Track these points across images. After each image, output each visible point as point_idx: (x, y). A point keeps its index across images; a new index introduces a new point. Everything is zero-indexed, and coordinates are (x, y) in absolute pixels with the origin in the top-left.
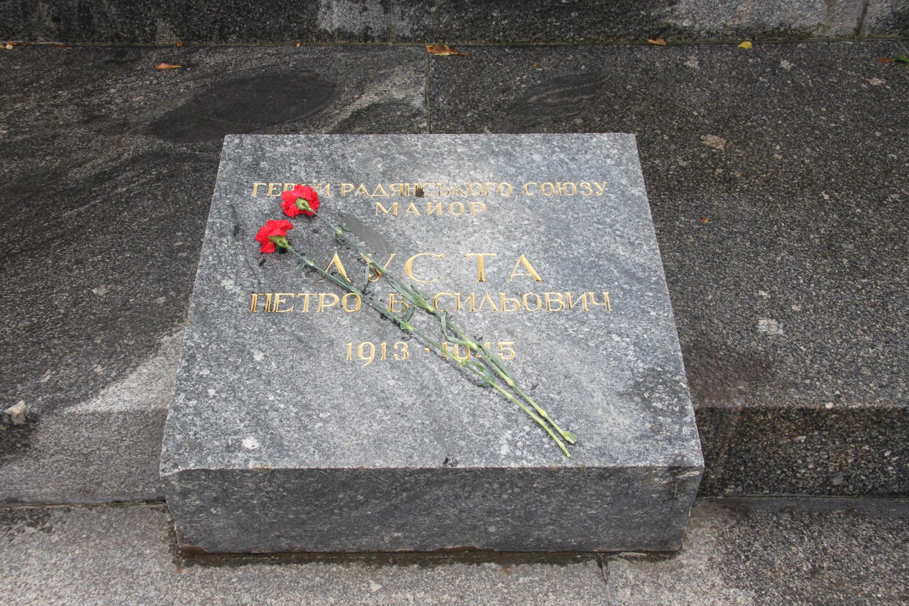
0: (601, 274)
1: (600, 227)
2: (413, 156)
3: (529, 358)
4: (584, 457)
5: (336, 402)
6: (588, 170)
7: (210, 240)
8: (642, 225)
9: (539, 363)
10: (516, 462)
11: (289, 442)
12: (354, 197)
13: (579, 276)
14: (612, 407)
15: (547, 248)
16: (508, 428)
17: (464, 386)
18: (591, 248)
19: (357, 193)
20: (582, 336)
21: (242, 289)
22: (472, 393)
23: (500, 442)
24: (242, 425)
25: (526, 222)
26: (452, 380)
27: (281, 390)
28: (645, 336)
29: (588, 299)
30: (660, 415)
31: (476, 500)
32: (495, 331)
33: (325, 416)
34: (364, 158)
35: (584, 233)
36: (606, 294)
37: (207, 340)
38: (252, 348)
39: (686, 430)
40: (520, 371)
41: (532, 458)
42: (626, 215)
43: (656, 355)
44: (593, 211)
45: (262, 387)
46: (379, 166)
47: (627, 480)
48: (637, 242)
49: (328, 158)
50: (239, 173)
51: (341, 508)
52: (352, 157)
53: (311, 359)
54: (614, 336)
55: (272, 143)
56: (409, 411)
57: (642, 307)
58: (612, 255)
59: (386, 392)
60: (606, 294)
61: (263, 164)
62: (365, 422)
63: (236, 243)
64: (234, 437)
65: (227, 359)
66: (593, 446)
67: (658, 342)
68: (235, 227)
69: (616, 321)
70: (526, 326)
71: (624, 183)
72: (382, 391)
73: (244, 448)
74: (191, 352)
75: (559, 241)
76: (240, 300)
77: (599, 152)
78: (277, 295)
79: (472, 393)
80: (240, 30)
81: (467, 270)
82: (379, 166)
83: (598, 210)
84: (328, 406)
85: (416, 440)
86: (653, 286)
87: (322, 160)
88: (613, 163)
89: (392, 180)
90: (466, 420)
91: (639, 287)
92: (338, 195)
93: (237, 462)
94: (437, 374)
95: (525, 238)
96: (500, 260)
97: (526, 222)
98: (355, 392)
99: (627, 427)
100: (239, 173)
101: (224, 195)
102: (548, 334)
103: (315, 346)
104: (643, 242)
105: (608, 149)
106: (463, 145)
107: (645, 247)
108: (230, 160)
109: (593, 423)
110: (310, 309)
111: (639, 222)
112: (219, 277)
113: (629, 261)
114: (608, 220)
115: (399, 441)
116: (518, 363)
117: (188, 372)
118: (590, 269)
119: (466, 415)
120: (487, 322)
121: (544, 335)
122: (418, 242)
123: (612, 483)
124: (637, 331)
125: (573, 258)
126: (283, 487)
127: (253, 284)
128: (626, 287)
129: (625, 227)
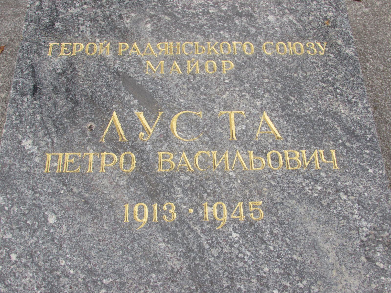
0: (327, 132)
1: (325, 85)
2: (175, 16)
5: (117, 266)
6: (311, 31)
7: (14, 100)
8: (356, 84)
9: (283, 224)
12: (129, 56)
14: (344, 268)
15: (284, 106)
17: (222, 248)
19: (131, 52)
20: (316, 195)
21: (38, 149)
22: (229, 255)
25: (267, 80)
26: (213, 242)
27: (71, 255)
28: (366, 194)
30: (382, 275)
32: (247, 191)
33: (108, 282)
34: (137, 18)
35: (313, 91)
36: (333, 152)
37: (10, 202)
38: (47, 210)
40: (268, 231)
42: (343, 74)
43: (376, 214)
44: (318, 70)
46: (149, 26)
48: (354, 100)
49: (108, 18)
50: (39, 33)
52: (127, 18)
53: (96, 221)
54: (341, 194)
55: (65, 5)
56: (178, 276)
57: (362, 164)
58: (335, 113)
59: (158, 255)
60: (333, 152)
62: (141, 288)
63: (35, 102)
68: (34, 86)
69: (342, 179)
70: (271, 185)
71: (339, 43)
72: (155, 255)
75: (293, 98)
76: (37, 160)
77: (318, 14)
78: (67, 154)
79: (229, 255)
81: (221, 128)
82: (149, 26)
83: (322, 69)
84: (109, 271)
86: (369, 144)
87: (104, 21)
90: (226, 285)
94: (200, 236)
96: (247, 118)
97: (267, 80)
98: (132, 256)
99: (357, 288)
100: (39, 33)
101: (26, 55)
102: (289, 193)
103: (98, 208)
104: (358, 101)
105: (325, 12)
106: (214, 7)
107: (360, 105)
108: (32, 21)
110: (94, 169)
111: (353, 81)
112: (20, 137)
113: (348, 119)
114: (330, 79)
116: (266, 224)
118: (319, 126)
119: (226, 279)
120: (239, 181)
121: (286, 194)
122: (181, 100)
124: (359, 189)
125: (306, 116)
127: (47, 144)
128: (348, 144)
129: (343, 85)
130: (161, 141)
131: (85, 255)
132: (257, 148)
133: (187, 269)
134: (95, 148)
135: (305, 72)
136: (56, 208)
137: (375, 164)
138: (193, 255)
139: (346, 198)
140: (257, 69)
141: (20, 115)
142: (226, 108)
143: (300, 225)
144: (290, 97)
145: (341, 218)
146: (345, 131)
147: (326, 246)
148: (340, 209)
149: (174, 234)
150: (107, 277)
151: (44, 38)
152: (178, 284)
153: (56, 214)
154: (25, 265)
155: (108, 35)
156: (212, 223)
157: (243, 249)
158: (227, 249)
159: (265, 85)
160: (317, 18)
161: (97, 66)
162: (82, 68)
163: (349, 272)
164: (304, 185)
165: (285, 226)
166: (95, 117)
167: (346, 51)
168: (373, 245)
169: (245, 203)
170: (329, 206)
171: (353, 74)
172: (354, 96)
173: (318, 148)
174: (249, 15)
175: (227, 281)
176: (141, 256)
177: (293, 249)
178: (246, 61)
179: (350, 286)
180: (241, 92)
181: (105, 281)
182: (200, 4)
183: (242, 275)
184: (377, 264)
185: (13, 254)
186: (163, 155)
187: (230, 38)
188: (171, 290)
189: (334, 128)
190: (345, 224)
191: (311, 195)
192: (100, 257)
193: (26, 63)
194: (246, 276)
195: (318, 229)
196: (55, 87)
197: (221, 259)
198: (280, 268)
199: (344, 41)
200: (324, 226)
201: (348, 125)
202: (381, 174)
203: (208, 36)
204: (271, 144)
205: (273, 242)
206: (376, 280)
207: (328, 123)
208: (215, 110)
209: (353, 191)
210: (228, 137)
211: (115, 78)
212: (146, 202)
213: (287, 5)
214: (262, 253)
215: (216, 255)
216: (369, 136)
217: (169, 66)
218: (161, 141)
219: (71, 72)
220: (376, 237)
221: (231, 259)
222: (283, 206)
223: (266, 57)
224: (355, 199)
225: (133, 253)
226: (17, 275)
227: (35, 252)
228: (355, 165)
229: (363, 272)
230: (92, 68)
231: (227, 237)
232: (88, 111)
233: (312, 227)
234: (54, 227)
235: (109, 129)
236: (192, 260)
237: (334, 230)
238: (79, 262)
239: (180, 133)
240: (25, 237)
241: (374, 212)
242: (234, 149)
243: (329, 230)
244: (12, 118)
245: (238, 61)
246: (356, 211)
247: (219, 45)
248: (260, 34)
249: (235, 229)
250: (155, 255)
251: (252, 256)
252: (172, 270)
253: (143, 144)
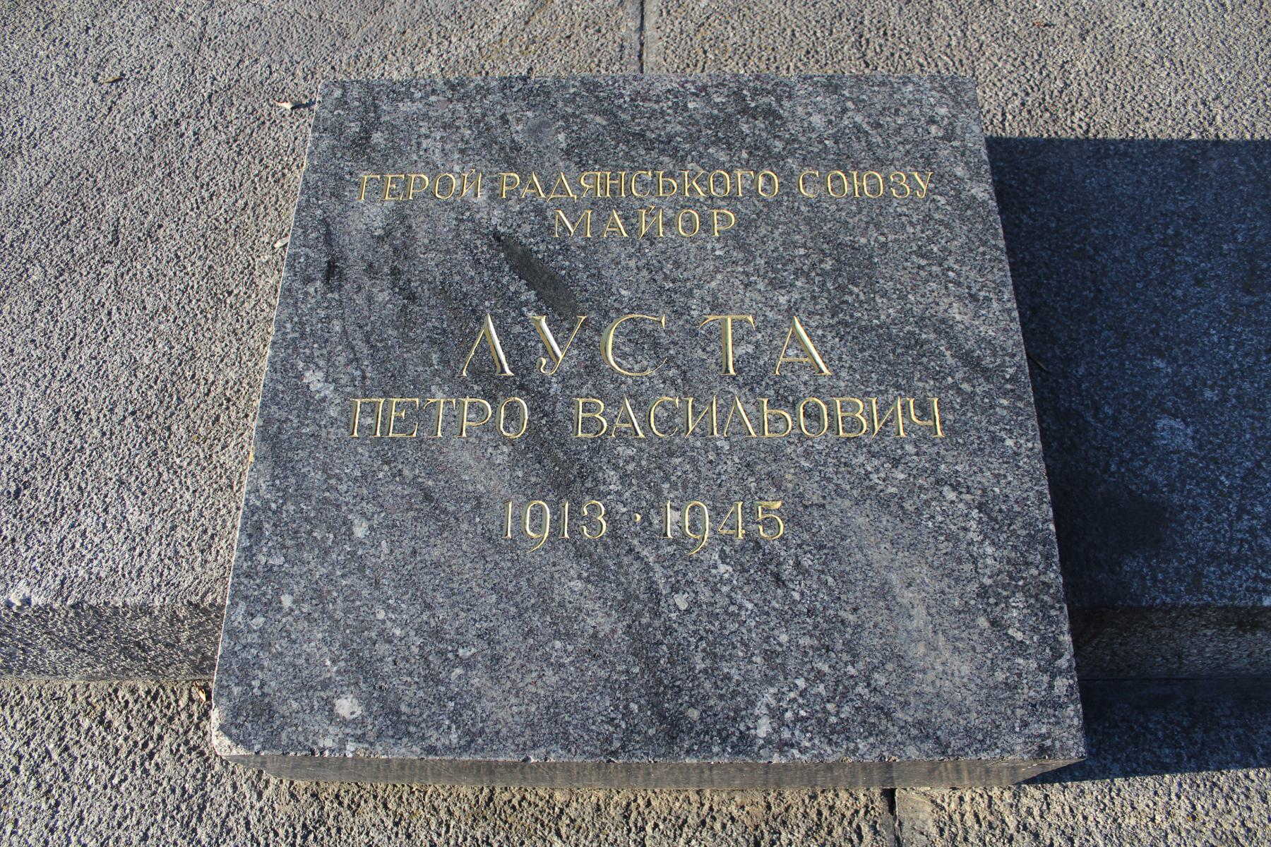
0: (925, 360)
1: (923, 262)
3: (806, 536)
4: (893, 741)
5: (485, 625)
6: (900, 148)
7: (289, 290)
8: (990, 260)
9: (822, 547)
10: (782, 752)
11: (409, 705)
13: (889, 363)
14: (941, 638)
15: (837, 306)
16: (770, 681)
17: (696, 593)
18: (909, 306)
20: (894, 490)
21: (336, 390)
22: (710, 609)
23: (757, 712)
24: (335, 669)
25: (802, 251)
28: (997, 490)
30: (1019, 655)
32: (751, 479)
33: (468, 654)
34: (537, 121)
37: (281, 494)
38: (351, 511)
39: (1061, 684)
40: (791, 562)
41: (808, 744)
45: (365, 593)
48: (983, 293)
49: (479, 122)
50: (339, 155)
52: (518, 120)
54: (946, 488)
56: (606, 646)
57: (992, 428)
58: (943, 321)
61: (377, 137)
62: (533, 667)
63: (329, 295)
64: (322, 694)
66: (910, 720)
67: (1016, 502)
68: (329, 262)
69: (950, 460)
70: (802, 468)
71: (959, 174)
72: (561, 605)
73: (338, 716)
74: (255, 518)
75: (856, 290)
76: (333, 412)
77: (917, 111)
79: (710, 609)
81: (704, 350)
82: (561, 137)
84: (471, 634)
85: (617, 708)
86: (1009, 386)
88: (940, 134)
89: (582, 165)
91: (987, 387)
92: (494, 196)
94: (652, 569)
95: (799, 284)
99: (965, 680)
100: (339, 155)
103: (451, 509)
104: (992, 295)
107: (995, 304)
108: (325, 130)
109: (907, 671)
111: (984, 254)
113: (969, 333)
114: (935, 250)
115: (589, 709)
117: (251, 560)
120: (737, 460)
121: (831, 487)
122: (623, 292)
124: (984, 480)
125: (880, 326)
127: (353, 380)
128: (966, 387)
129: (962, 263)
130: (580, 375)
131: (425, 602)
132: (777, 392)
133: (624, 633)
134: (447, 389)
135: (883, 234)
136: (370, 508)
137: (1020, 428)
138: (638, 606)
139: (954, 498)
140: (781, 228)
141: (300, 322)
142: (717, 307)
143: (856, 550)
144: (850, 286)
145: (942, 538)
146: (960, 359)
147: (908, 594)
148: (940, 519)
149: (598, 563)
150: (464, 645)
151: (350, 164)
152: (605, 662)
153: (369, 520)
155: (477, 158)
156: (678, 544)
157: (739, 597)
158: (705, 595)
159: (798, 262)
160: (913, 120)
161: (454, 222)
162: (425, 226)
163: (952, 648)
164: (869, 469)
165: (826, 551)
166: (448, 326)
167: (973, 191)
168: (1005, 593)
169: (747, 504)
170: (918, 511)
171: (984, 238)
172: (984, 286)
173: (903, 393)
174: (770, 113)
175: (703, 660)
176: (533, 605)
177: (839, 598)
178: (761, 211)
179: (952, 674)
180: (747, 274)
181: (461, 652)
182: (669, 91)
183: (734, 648)
184: (1010, 632)
185: (287, 596)
186: (584, 404)
187: (730, 161)
188: (590, 673)
189: (937, 351)
190: (949, 550)
191: (882, 491)
192: (452, 606)
193: (313, 217)
194: (742, 651)
195: (893, 560)
196: (371, 265)
197: (694, 616)
198: (811, 636)
199: (969, 169)
200: (906, 554)
201: (967, 347)
202: (1031, 449)
203: (683, 159)
204: (805, 384)
205: (800, 584)
206: (1007, 664)
207: (928, 341)
208: (692, 312)
209: (970, 484)
210: (718, 368)
211: (490, 246)
212: (548, 498)
213: (851, 93)
214: (777, 606)
215: (683, 606)
216: (1011, 371)
217: (600, 221)
218: (580, 375)
219: (403, 234)
220: (1011, 578)
221: (713, 616)
222: (824, 512)
223: (803, 203)
224: (973, 500)
225: (518, 599)
226: (293, 637)
227: (329, 592)
228: (977, 430)
229: (979, 648)
230: (445, 227)
231: (708, 571)
232: (434, 313)
233: (880, 554)
234: (365, 544)
235: (476, 352)
236: (635, 616)
237: (927, 563)
238: (411, 613)
239: (619, 360)
240: (309, 563)
241: (1012, 528)
242: (730, 392)
243: (915, 563)
244: (285, 327)
245: (744, 211)
246: (973, 524)
247: (706, 177)
248: (792, 153)
249: (724, 557)
250: (561, 605)
251: (756, 610)
252: (595, 636)
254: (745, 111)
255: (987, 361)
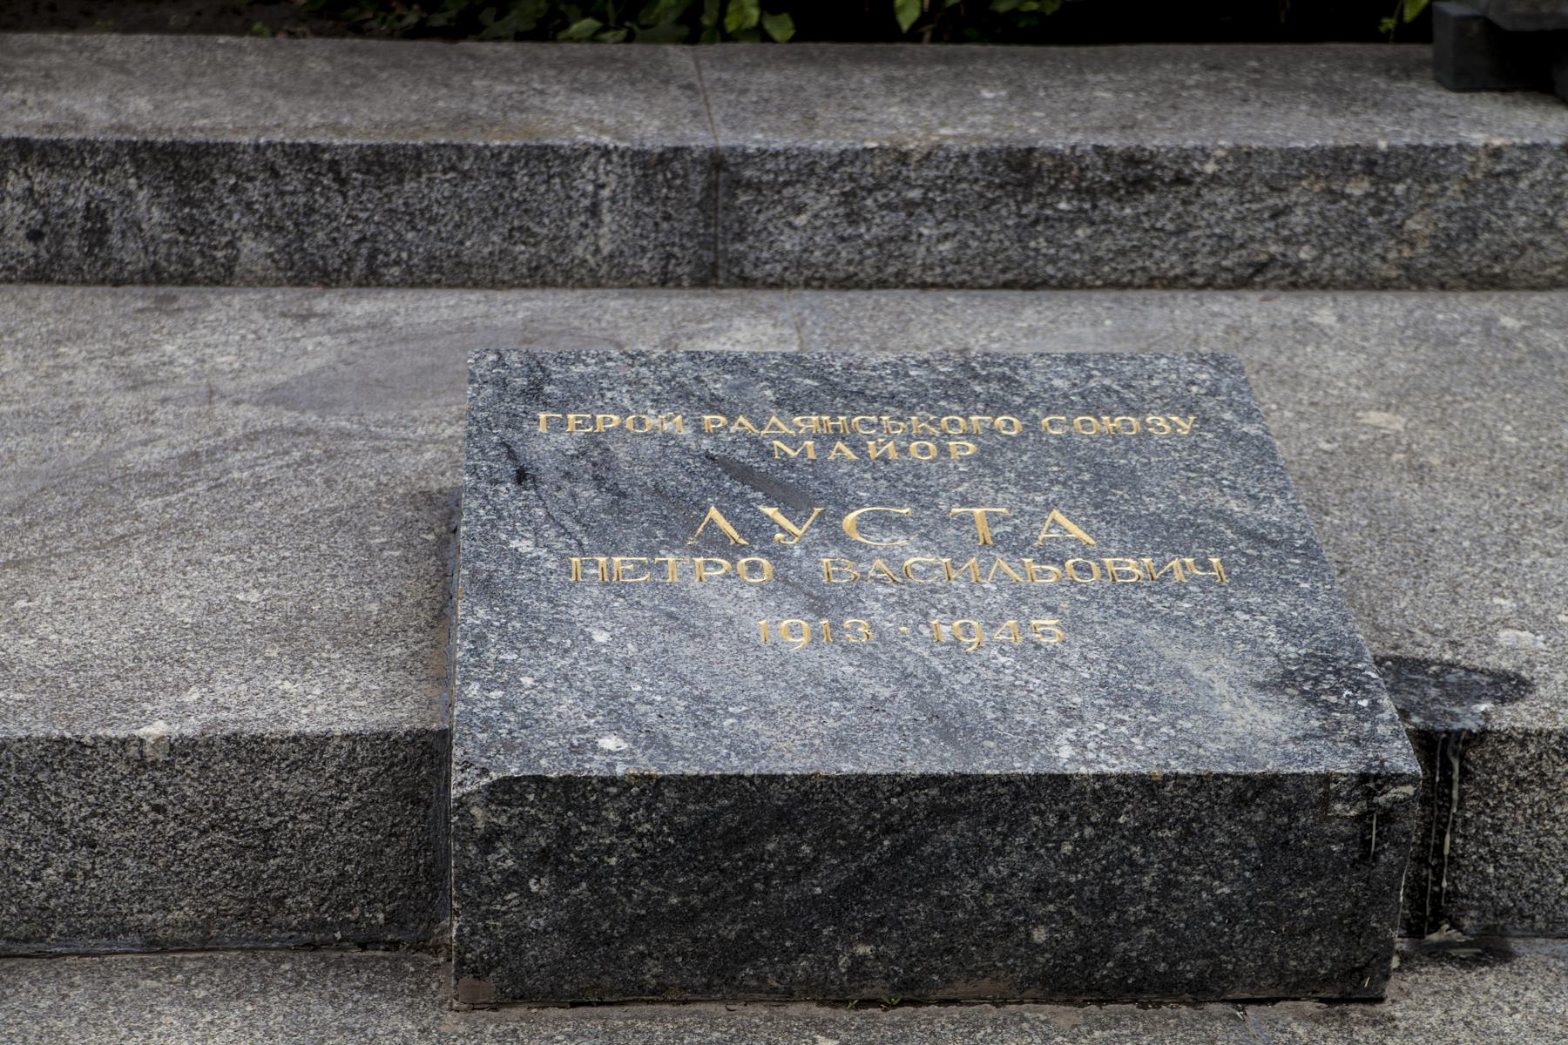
12: (730, 434)
29: (1181, 567)
31: (1015, 857)
47: (1288, 809)
51: (767, 878)
52: (715, 381)
54: (1237, 613)
65: (544, 639)
77: (1174, 376)
80: (410, 257)
84: (741, 698)
93: (595, 767)
103: (701, 624)
107: (1277, 501)
112: (504, 537)
118: (1182, 529)
123: (1259, 816)
126: (671, 824)
136: (609, 625)
154: (554, 690)
232: (651, 505)
233: (1174, 652)
235: (705, 529)
253: (785, 548)
254: (976, 376)
255: (1274, 535)
